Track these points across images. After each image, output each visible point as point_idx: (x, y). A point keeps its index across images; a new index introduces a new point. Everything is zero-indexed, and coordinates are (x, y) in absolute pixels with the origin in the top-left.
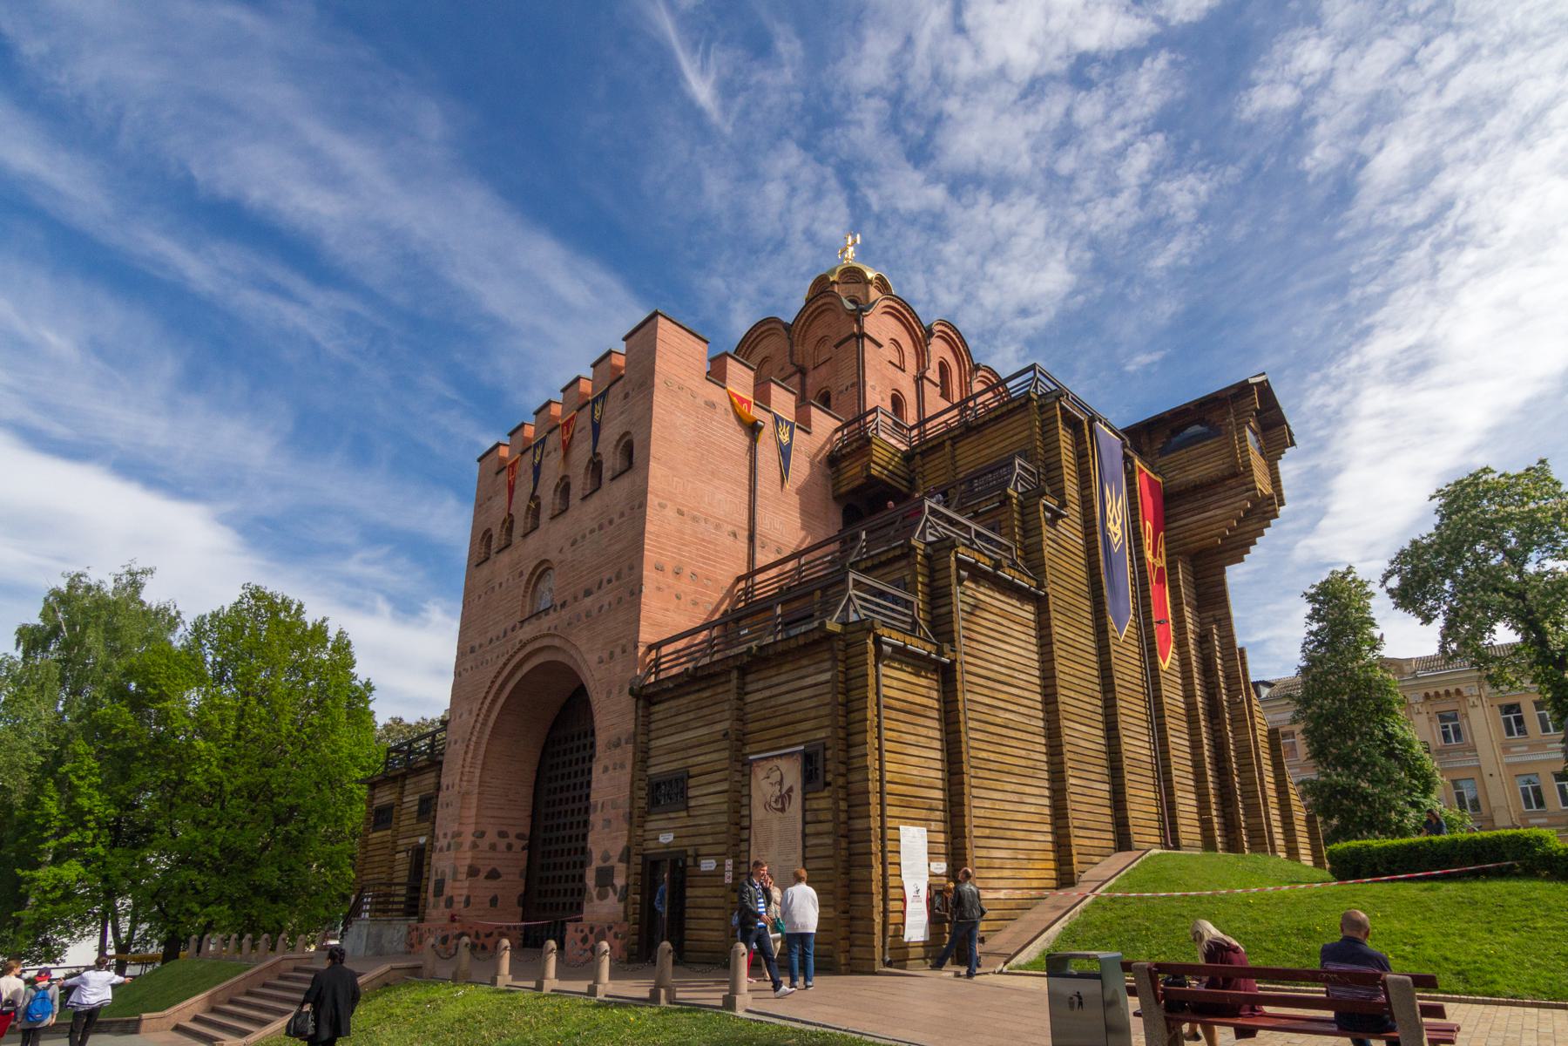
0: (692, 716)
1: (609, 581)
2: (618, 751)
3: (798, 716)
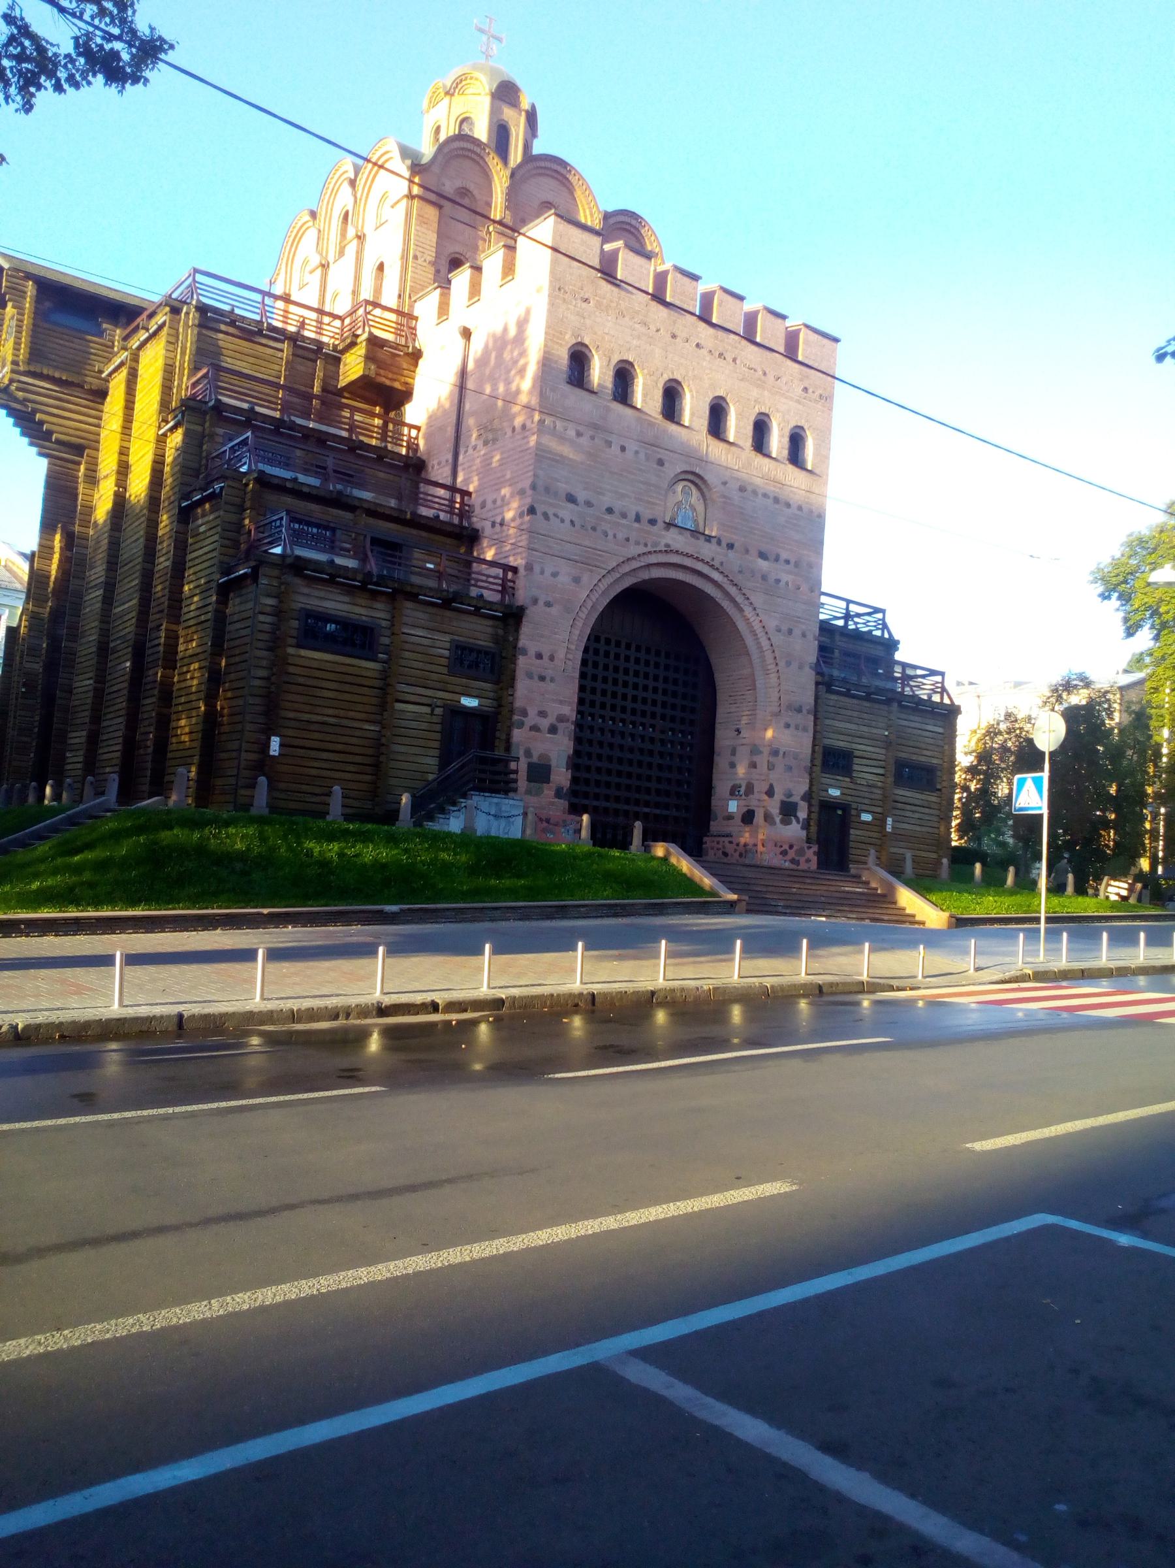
2: (800, 716)
3: (923, 746)
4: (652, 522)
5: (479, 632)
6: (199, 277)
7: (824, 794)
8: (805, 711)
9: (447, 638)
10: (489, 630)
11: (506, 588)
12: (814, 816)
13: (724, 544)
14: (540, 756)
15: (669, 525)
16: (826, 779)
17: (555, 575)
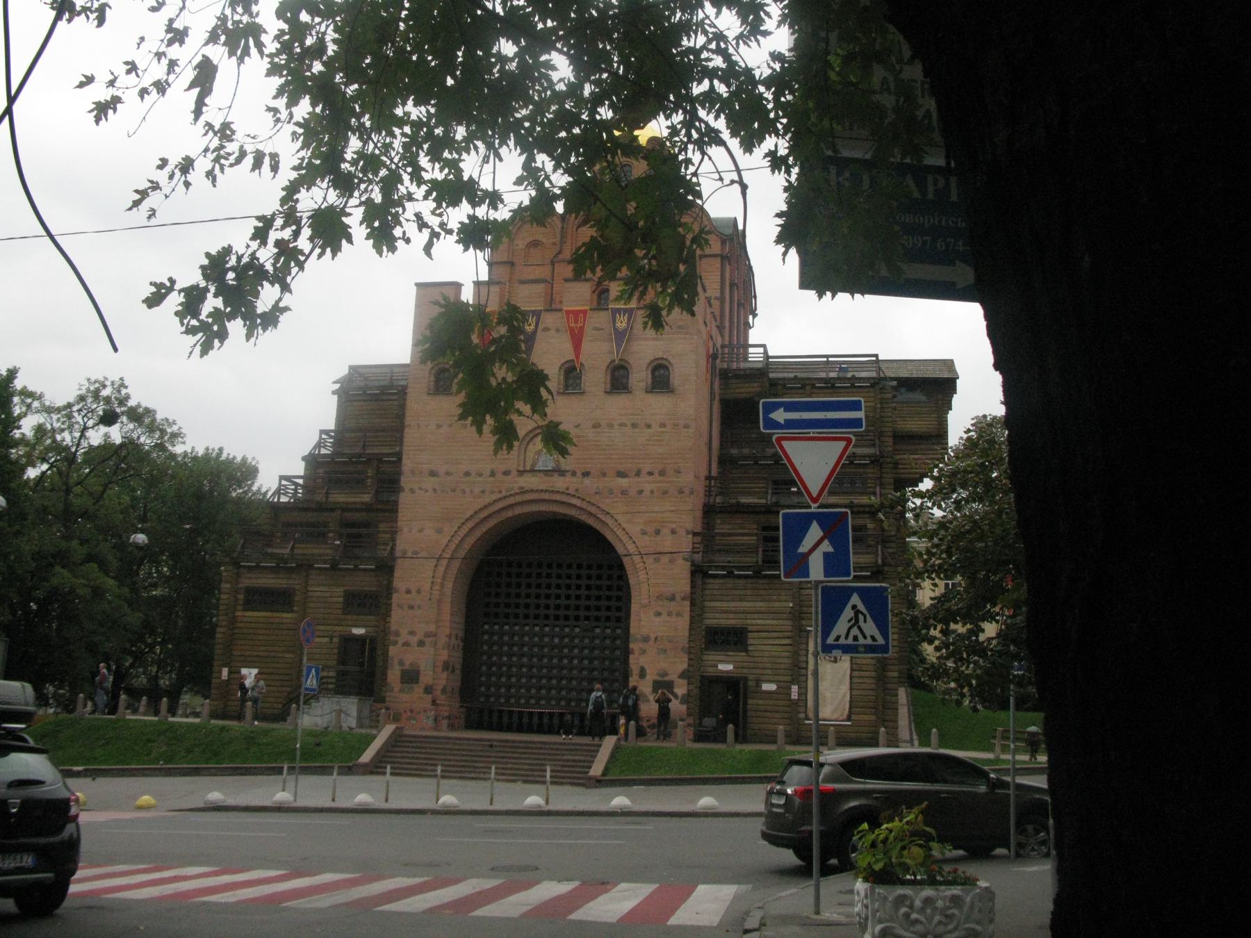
0: (749, 592)
1: (650, 474)
2: (673, 604)
4: (506, 473)
5: (365, 583)
7: (711, 669)
8: (678, 598)
12: (696, 691)
13: (579, 474)
14: (411, 664)
15: (521, 473)
16: (710, 657)
17: (421, 531)
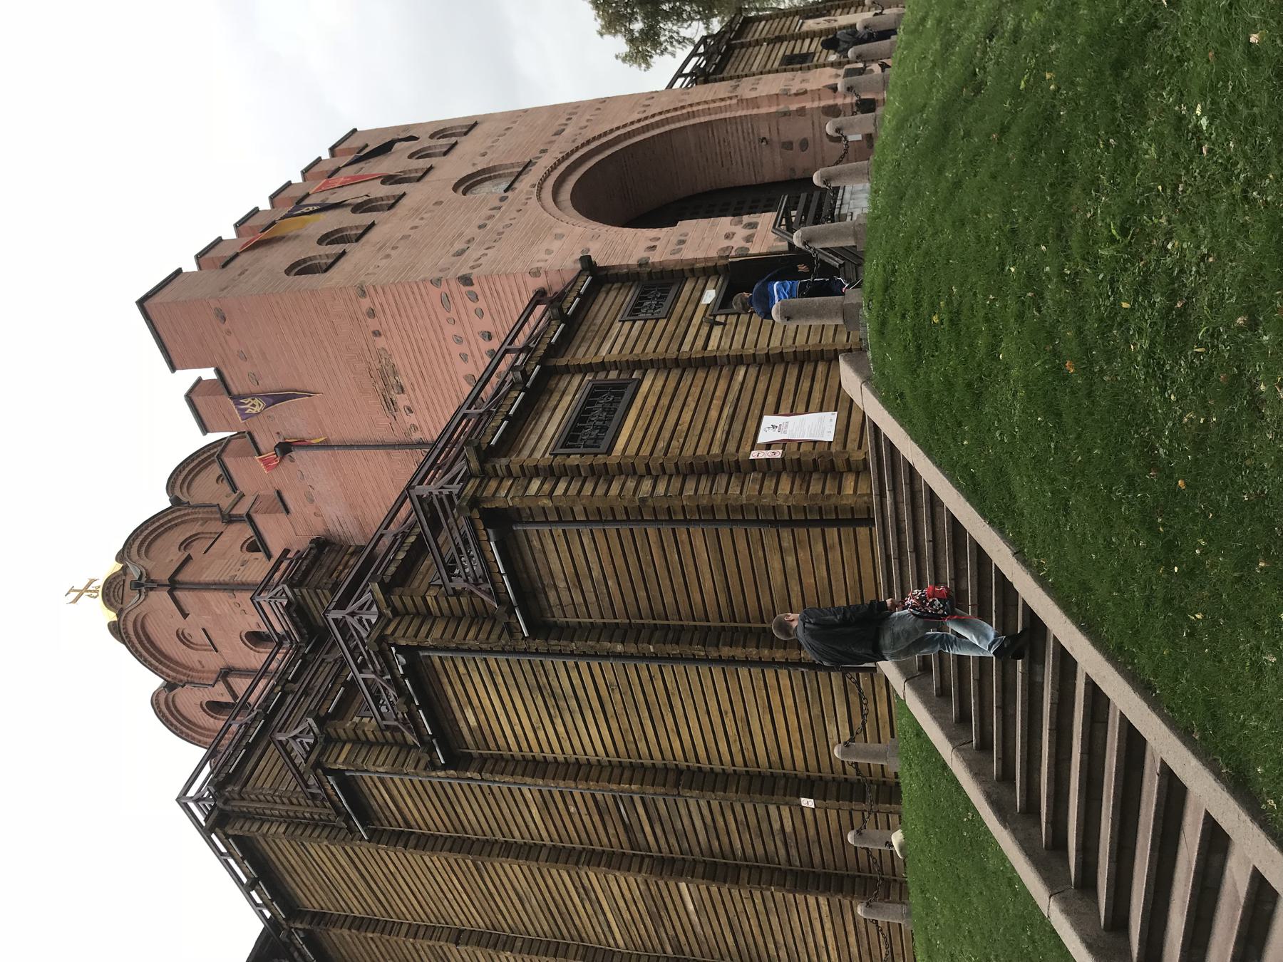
6: (192, 793)
9: (617, 325)
10: (613, 294)
11: (561, 297)
17: (548, 252)
